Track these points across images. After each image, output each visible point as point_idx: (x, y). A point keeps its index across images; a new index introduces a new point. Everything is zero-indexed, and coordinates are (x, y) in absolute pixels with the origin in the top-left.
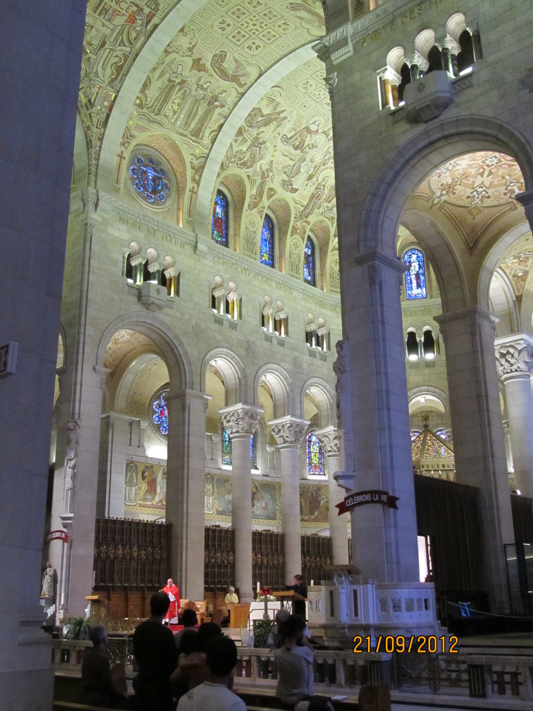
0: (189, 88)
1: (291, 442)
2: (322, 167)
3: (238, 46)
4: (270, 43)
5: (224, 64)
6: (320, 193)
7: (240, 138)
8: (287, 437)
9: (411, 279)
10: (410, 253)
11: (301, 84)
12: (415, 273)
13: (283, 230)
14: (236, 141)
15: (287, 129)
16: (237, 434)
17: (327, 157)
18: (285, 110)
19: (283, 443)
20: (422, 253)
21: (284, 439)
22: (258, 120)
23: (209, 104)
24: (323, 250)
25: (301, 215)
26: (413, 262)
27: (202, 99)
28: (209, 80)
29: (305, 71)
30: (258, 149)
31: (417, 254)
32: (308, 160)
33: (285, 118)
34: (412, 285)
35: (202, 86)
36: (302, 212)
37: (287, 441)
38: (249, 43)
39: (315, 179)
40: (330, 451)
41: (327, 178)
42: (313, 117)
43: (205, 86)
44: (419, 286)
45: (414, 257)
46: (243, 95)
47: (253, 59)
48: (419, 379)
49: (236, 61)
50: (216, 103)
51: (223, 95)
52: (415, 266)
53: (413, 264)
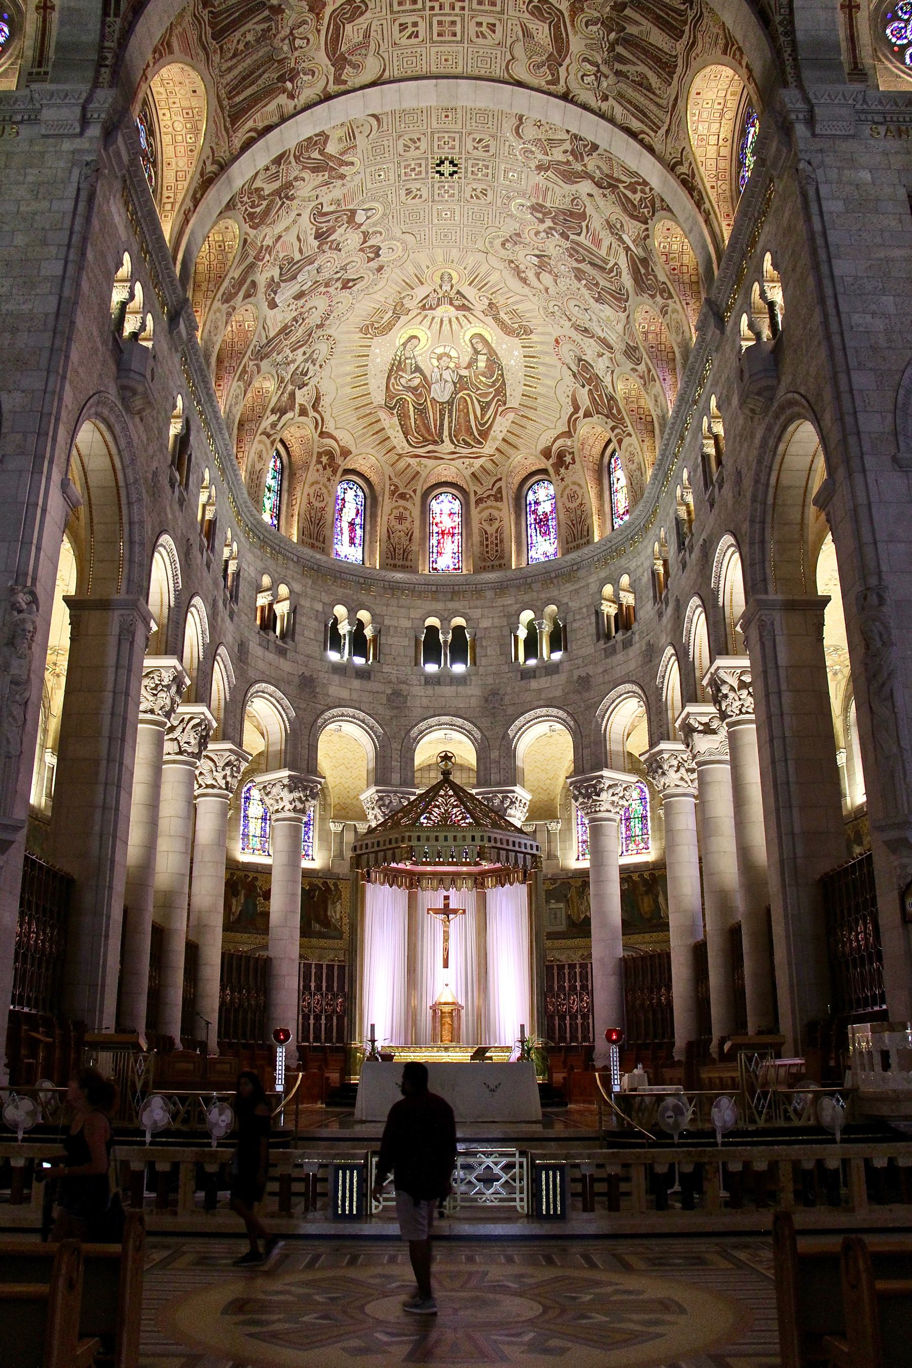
0: (277, 29)
1: (192, 755)
2: (323, 289)
3: (392, 12)
4: (436, 42)
5: (348, 27)
7: (273, 169)
8: (188, 743)
10: (346, 486)
11: (407, 137)
13: (226, 364)
14: (267, 169)
15: (329, 197)
16: (149, 716)
17: (339, 275)
18: (352, 164)
19: (177, 754)
21: (180, 747)
22: (312, 156)
23: (282, 79)
24: (246, 427)
27: (279, 61)
28: (310, 36)
29: (434, 118)
32: (316, 265)
33: (342, 177)
35: (294, 40)
37: (185, 751)
38: (409, 20)
39: (303, 301)
40: (213, 786)
42: (374, 200)
43: (298, 42)
44: (352, 542)
46: (328, 97)
47: (390, 49)
48: (345, 694)
49: (367, 35)
50: (289, 85)
51: (305, 78)
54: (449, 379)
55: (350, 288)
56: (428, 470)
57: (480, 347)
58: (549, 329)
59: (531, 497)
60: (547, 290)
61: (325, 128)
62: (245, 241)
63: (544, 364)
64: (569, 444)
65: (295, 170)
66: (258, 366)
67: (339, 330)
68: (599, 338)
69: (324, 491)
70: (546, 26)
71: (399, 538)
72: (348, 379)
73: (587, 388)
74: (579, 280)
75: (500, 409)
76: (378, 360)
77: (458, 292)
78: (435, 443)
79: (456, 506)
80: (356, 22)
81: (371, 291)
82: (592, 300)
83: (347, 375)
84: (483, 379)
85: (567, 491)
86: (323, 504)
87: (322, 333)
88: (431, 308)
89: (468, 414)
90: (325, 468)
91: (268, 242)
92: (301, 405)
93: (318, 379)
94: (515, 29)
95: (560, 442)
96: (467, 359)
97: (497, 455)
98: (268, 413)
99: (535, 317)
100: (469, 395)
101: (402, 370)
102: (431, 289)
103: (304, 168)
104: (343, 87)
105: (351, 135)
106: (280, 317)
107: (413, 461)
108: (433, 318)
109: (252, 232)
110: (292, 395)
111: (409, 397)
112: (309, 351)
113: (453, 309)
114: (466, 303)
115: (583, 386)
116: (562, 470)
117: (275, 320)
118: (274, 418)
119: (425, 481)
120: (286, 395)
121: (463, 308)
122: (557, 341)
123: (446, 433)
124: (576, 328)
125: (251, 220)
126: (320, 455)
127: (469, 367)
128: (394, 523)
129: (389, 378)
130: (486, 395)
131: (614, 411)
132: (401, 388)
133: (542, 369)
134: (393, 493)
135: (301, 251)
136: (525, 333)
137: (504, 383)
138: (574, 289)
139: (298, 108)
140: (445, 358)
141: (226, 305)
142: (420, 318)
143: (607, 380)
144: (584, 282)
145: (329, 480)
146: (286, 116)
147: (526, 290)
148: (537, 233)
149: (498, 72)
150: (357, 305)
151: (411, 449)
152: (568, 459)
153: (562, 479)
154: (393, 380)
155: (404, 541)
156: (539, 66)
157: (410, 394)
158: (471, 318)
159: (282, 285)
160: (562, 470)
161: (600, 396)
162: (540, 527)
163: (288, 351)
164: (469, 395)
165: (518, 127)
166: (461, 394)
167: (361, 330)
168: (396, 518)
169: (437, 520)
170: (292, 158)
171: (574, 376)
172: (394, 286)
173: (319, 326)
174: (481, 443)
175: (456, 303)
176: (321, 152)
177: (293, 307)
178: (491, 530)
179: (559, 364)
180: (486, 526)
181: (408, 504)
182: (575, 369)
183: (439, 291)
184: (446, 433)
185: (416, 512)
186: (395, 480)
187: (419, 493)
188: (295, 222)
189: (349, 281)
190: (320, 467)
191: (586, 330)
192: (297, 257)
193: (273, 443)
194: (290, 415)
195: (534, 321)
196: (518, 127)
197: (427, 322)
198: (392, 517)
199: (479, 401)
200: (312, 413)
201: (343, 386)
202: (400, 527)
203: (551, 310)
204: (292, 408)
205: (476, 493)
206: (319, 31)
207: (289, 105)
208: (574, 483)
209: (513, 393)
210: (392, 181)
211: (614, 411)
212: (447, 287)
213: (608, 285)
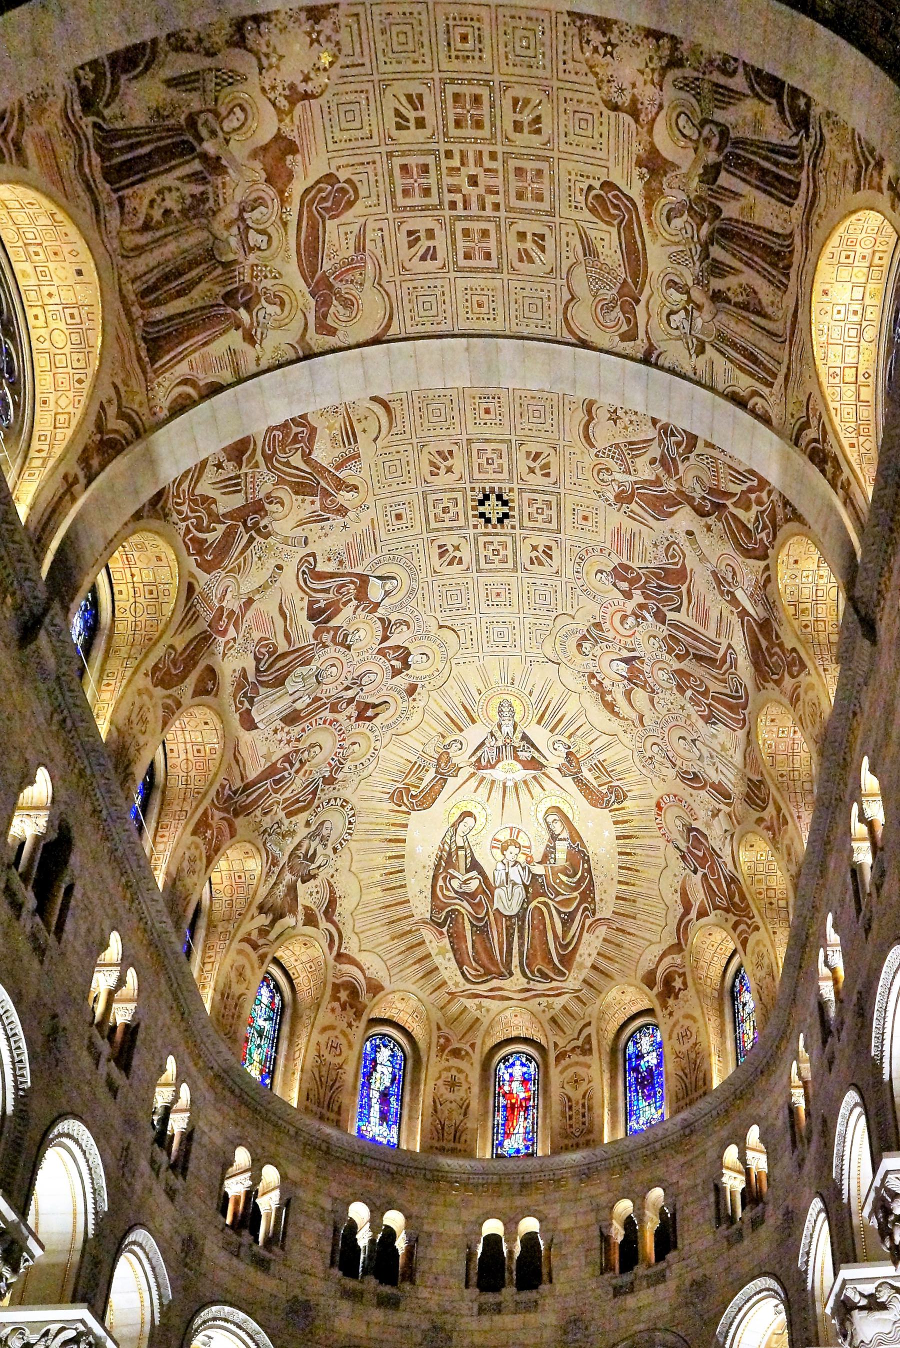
6: (286, 773)
7: (230, 469)
30: (246, 537)
56: (492, 1014)
60: (641, 717)
61: (309, 408)
62: (191, 588)
65: (265, 483)
66: (231, 826)
70: (614, 231)
80: (343, 219)
83: (374, 869)
91: (231, 603)
93: (332, 871)
94: (572, 244)
103: (281, 481)
104: (332, 341)
105: (350, 436)
106: (263, 750)
109: (203, 578)
119: (487, 1033)
125: (200, 552)
129: (435, 878)
135: (287, 636)
139: (264, 364)
141: (159, 692)
146: (244, 374)
148: (624, 618)
149: (555, 328)
154: (440, 882)
156: (608, 308)
163: (282, 814)
165: (586, 427)
166: (531, 906)
170: (259, 457)
176: (307, 457)
181: (463, 1064)
188: (273, 579)
192: (283, 646)
196: (586, 427)
201: (369, 887)
206: (285, 224)
207: (249, 357)
210: (417, 530)
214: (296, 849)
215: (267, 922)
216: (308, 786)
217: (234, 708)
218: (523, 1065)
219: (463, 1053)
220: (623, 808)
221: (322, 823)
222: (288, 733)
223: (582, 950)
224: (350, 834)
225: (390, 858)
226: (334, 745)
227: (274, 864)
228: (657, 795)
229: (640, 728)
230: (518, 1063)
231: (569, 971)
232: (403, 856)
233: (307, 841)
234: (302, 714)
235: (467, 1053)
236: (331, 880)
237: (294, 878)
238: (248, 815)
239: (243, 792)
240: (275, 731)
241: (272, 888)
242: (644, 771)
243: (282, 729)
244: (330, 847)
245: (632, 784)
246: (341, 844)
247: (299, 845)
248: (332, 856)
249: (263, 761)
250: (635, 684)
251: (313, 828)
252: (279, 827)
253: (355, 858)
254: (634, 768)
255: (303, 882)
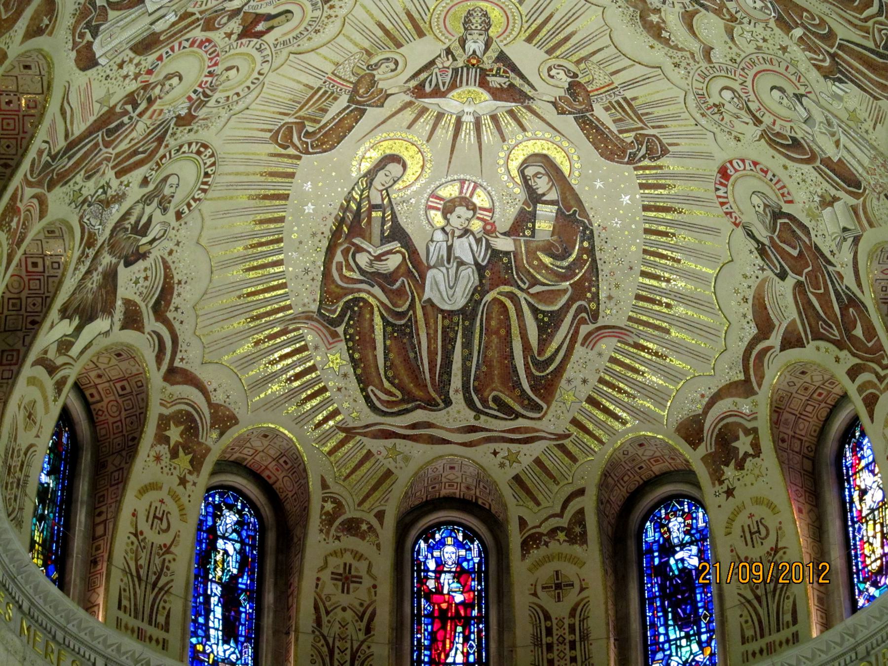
2: (198, 34)
6: (126, 119)
9: (207, 598)
12: (225, 578)
20: (258, 514)
25: (47, 165)
26: (224, 537)
31: (239, 512)
34: (207, 619)
36: (54, 158)
39: (152, 58)
41: (175, 81)
45: (231, 518)
52: (226, 552)
53: (220, 543)
54: (469, 259)
55: (259, 35)
56: (413, 467)
57: (542, 185)
58: (708, 144)
59: (651, 535)
60: (707, 52)
63: (690, 226)
64: (746, 409)
66: (42, 202)
67: (227, 132)
68: (827, 162)
69: (171, 506)
71: (343, 625)
72: (239, 249)
73: (791, 280)
74: (786, 26)
75: (584, 330)
76: (309, 208)
77: (502, 58)
78: (430, 405)
79: (474, 554)
81: (306, 45)
82: (814, 75)
83: (237, 238)
84: (547, 260)
85: (743, 519)
86: (166, 539)
87: (191, 137)
88: (437, 93)
89: (507, 340)
90: (174, 454)
92: (127, 302)
93: (171, 245)
95: (724, 405)
96: (512, 213)
97: (573, 430)
98: (54, 314)
99: (675, 117)
100: (512, 297)
101: (362, 234)
102: (439, 48)
106: (98, 92)
107: (377, 445)
108: (440, 116)
110: (111, 277)
111: (375, 295)
112: (156, 177)
113: (486, 95)
114: (518, 82)
115: (782, 276)
116: (730, 472)
117: (89, 96)
118: (65, 328)
120: (96, 277)
121: (511, 93)
122: (724, 173)
123: (456, 382)
124: (772, 139)
126: (164, 422)
127: (514, 231)
128: (330, 588)
129: (330, 251)
130: (550, 296)
131: (858, 332)
132: (356, 275)
133: (685, 238)
134: (329, 519)
136: (651, 154)
137: (594, 269)
138: (771, 47)
140: (461, 210)
142: (408, 115)
143: (842, 260)
144: (798, 32)
145: (183, 482)
147: (659, 54)
150: (271, 77)
151: (374, 418)
152: (743, 445)
153: (730, 493)
154: (339, 257)
155: (355, 632)
157: (377, 291)
158: (527, 118)
159: (112, 14)
160: (730, 472)
161: (824, 299)
162: (675, 605)
163: (110, 174)
164: (512, 297)
167: (274, 139)
168: (336, 576)
169: (431, 584)
171: (762, 251)
172: (357, 37)
173: (186, 120)
174: (538, 408)
175: (495, 81)
177: (130, 69)
178: (559, 610)
179: (726, 225)
180: (546, 600)
182: (763, 234)
183: (458, 52)
184: (456, 382)
185: (384, 564)
186: (334, 488)
187: (390, 521)
189: (259, 18)
190: (163, 449)
191: (796, 144)
193: (59, 386)
194: (101, 324)
195: (673, 126)
197: (424, 125)
198: (326, 576)
199: (535, 311)
200: (151, 323)
201: (226, 264)
202: (344, 599)
203: (715, 99)
204: (108, 309)
205: (522, 522)
208: (758, 501)
209: (614, 293)
211: (858, 332)
212: (475, 45)
213: (855, 36)
214: (124, 218)
215: (70, 331)
216: (153, 131)
217: (70, 45)
218: (459, 545)
219: (364, 527)
220: (660, 167)
221: (165, 179)
222: (137, 65)
223: (569, 373)
224: (204, 191)
225: (262, 222)
226: (201, 70)
227: (90, 244)
228: (721, 157)
229: (704, 64)
230: (449, 541)
231: (548, 407)
232: (281, 220)
233: (141, 205)
234: (162, 38)
235: (371, 528)
236: (169, 259)
237: (114, 260)
238: (66, 183)
239: (65, 153)
240: (121, 66)
241: (83, 278)
242: (703, 121)
243: (131, 61)
244: (171, 214)
245: (679, 136)
246: (189, 205)
247: (128, 213)
248: (174, 223)
249: (97, 106)
250: (702, 5)
251: (151, 187)
252: (105, 192)
253: (208, 222)
254: (687, 115)
255: (128, 264)
